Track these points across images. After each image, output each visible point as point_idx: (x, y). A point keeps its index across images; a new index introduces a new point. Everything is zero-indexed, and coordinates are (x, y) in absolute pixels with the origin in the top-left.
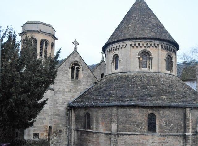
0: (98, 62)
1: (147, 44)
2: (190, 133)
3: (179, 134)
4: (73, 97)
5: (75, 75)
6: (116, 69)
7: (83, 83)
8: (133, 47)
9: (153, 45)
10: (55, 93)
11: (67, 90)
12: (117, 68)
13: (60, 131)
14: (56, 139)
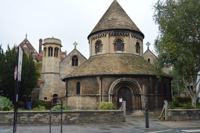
9: (102, 36)
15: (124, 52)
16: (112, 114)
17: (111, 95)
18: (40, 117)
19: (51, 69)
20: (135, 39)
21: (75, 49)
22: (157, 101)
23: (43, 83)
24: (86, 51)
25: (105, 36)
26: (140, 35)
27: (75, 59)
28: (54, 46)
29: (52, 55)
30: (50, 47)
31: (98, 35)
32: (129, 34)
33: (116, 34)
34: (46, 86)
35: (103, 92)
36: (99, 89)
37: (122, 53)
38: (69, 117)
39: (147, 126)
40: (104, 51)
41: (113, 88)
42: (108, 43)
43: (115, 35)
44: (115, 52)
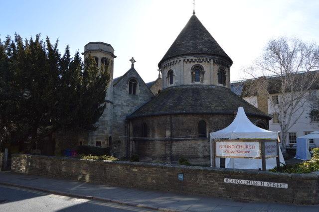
0: (155, 79)
1: (199, 59)
4: (131, 110)
5: (133, 91)
6: (171, 84)
7: (140, 98)
8: (186, 62)
10: (114, 106)
12: (171, 83)
13: (119, 142)
14: (115, 149)
15: (225, 87)
21: (132, 70)
28: (109, 57)
42: (212, 72)
44: (218, 85)
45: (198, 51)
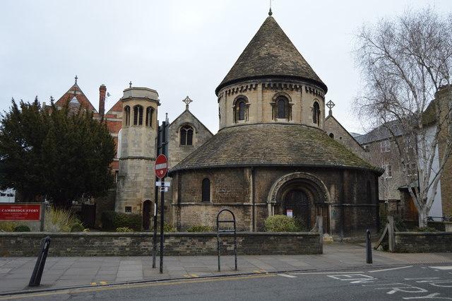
2: (252, 204)
3: (237, 203)
11: (175, 159)
15: (290, 122)
16: (299, 240)
17: (272, 204)
18: (175, 244)
19: (140, 151)
20: (312, 95)
21: (187, 111)
22: (355, 217)
23: (123, 177)
24: (210, 117)
25: (255, 89)
26: (319, 87)
27: (188, 127)
28: (145, 105)
29: (141, 123)
30: (138, 105)
31: (239, 87)
32: (301, 87)
33: (278, 85)
34: (130, 185)
35: (257, 198)
36: (249, 192)
37: (287, 122)
38: (225, 243)
39: (370, 260)
40: (252, 118)
41: (276, 192)
42: (260, 102)
43: (274, 88)
44: (273, 121)
45: (240, 76)
